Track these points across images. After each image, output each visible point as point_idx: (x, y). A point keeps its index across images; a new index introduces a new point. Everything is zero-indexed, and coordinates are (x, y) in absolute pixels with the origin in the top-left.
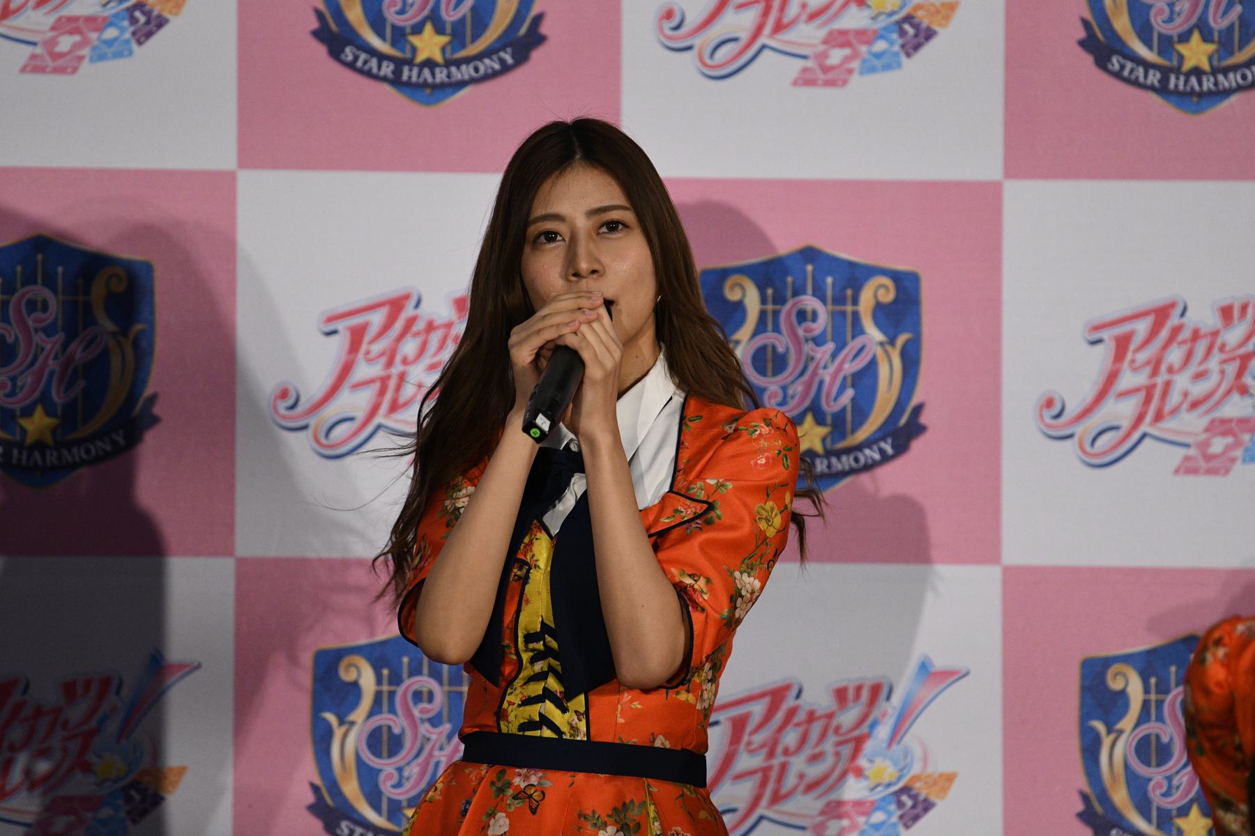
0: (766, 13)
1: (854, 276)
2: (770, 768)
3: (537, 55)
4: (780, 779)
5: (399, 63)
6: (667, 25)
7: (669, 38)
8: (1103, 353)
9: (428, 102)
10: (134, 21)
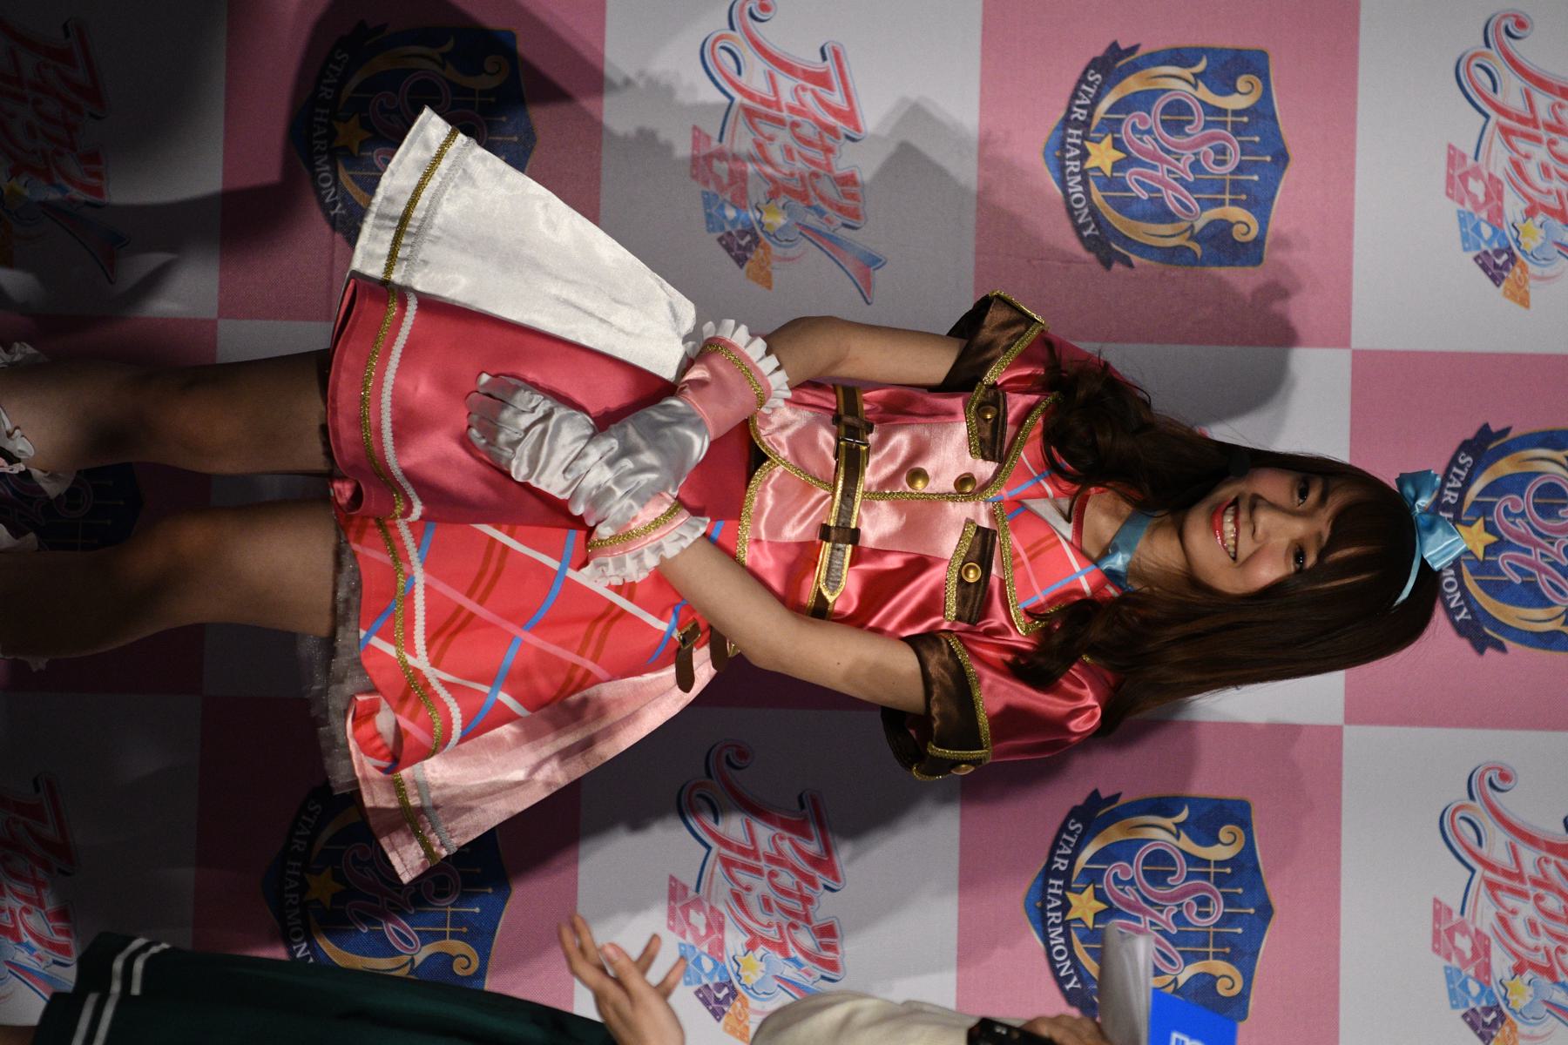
1: (1243, 954)
2: (757, 858)
3: (1464, 644)
4: (746, 867)
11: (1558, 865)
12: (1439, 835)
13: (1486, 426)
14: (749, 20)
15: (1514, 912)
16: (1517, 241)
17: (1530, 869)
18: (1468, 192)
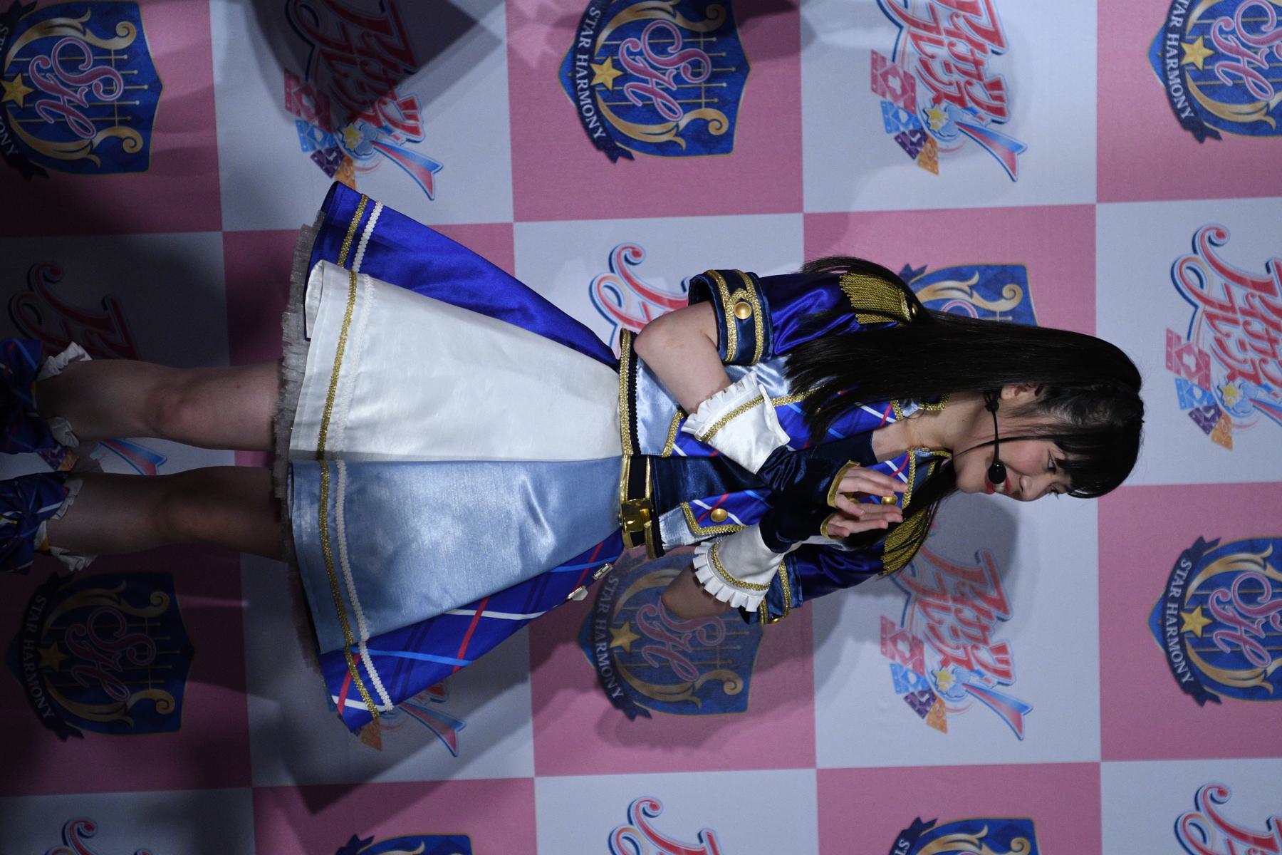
0: (1222, 307)
3: (1189, 699)
5: (1180, 601)
6: (1212, 234)
7: (1205, 793)
8: (968, 561)
9: (1151, 54)
10: (1207, 409)
11: (1260, 297)
12: (1173, 836)
13: (1201, 539)
14: (624, 264)
15: (1228, 335)
16: (1221, 399)
17: (1239, 302)
18: (1183, 364)
